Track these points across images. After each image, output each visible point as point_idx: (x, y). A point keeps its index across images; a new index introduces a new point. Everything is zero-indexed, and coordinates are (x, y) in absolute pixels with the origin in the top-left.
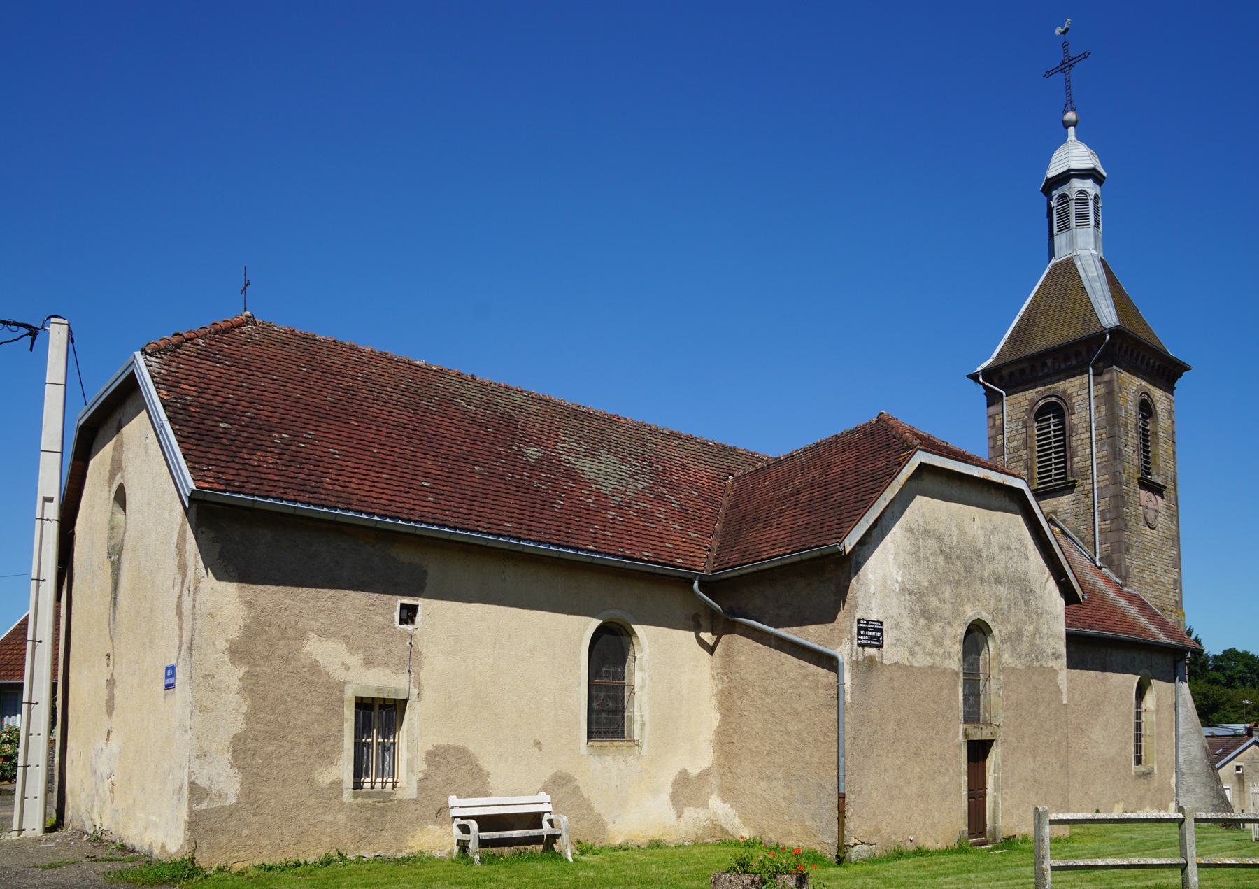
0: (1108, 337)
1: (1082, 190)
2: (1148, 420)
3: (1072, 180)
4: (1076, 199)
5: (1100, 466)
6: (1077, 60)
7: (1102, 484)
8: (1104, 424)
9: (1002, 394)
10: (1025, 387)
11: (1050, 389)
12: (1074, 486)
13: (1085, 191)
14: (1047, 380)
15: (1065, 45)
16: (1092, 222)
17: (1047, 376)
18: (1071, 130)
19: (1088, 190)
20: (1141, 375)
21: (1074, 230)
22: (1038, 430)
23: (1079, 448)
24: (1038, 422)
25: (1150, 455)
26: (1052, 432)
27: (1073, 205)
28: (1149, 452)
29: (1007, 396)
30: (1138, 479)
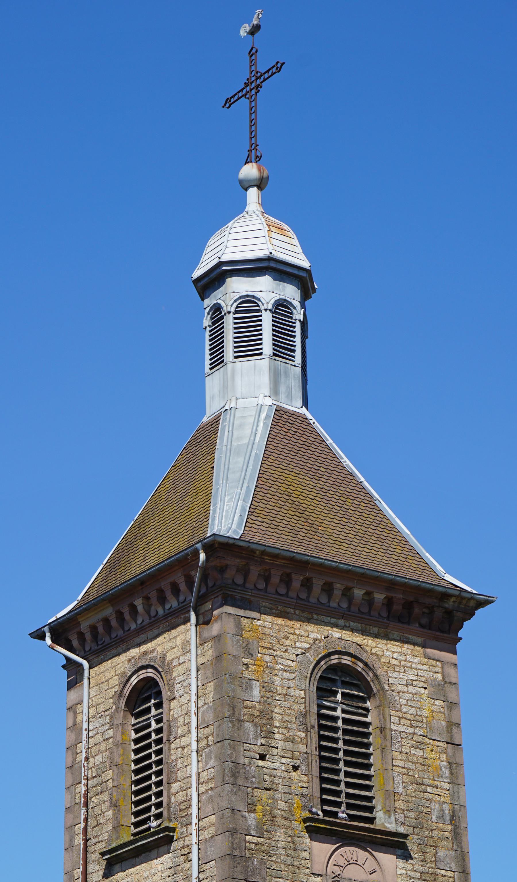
0: (202, 556)
1: (247, 296)
2: (369, 704)
3: (228, 280)
4: (236, 312)
5: (204, 798)
6: (266, 76)
7: (206, 835)
8: (210, 717)
9: (81, 665)
10: (114, 652)
11: (145, 653)
12: (170, 840)
13: (253, 297)
14: (142, 637)
15: (252, 53)
16: (267, 347)
17: (141, 630)
18: (253, 193)
19: (258, 295)
20: (327, 619)
21: (229, 366)
22: (137, 731)
23: (179, 765)
24: (138, 716)
25: (372, 772)
26: (153, 734)
27: (229, 322)
28: (372, 765)
29: (91, 668)
30: (305, 821)
